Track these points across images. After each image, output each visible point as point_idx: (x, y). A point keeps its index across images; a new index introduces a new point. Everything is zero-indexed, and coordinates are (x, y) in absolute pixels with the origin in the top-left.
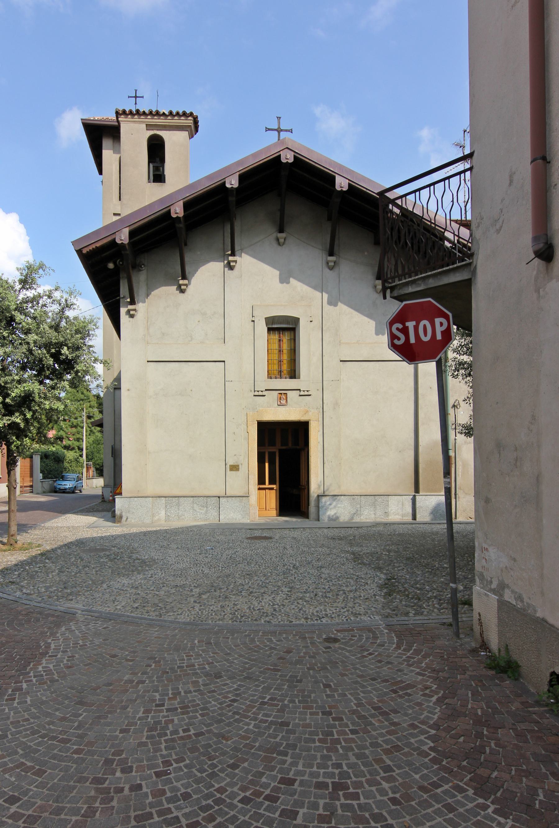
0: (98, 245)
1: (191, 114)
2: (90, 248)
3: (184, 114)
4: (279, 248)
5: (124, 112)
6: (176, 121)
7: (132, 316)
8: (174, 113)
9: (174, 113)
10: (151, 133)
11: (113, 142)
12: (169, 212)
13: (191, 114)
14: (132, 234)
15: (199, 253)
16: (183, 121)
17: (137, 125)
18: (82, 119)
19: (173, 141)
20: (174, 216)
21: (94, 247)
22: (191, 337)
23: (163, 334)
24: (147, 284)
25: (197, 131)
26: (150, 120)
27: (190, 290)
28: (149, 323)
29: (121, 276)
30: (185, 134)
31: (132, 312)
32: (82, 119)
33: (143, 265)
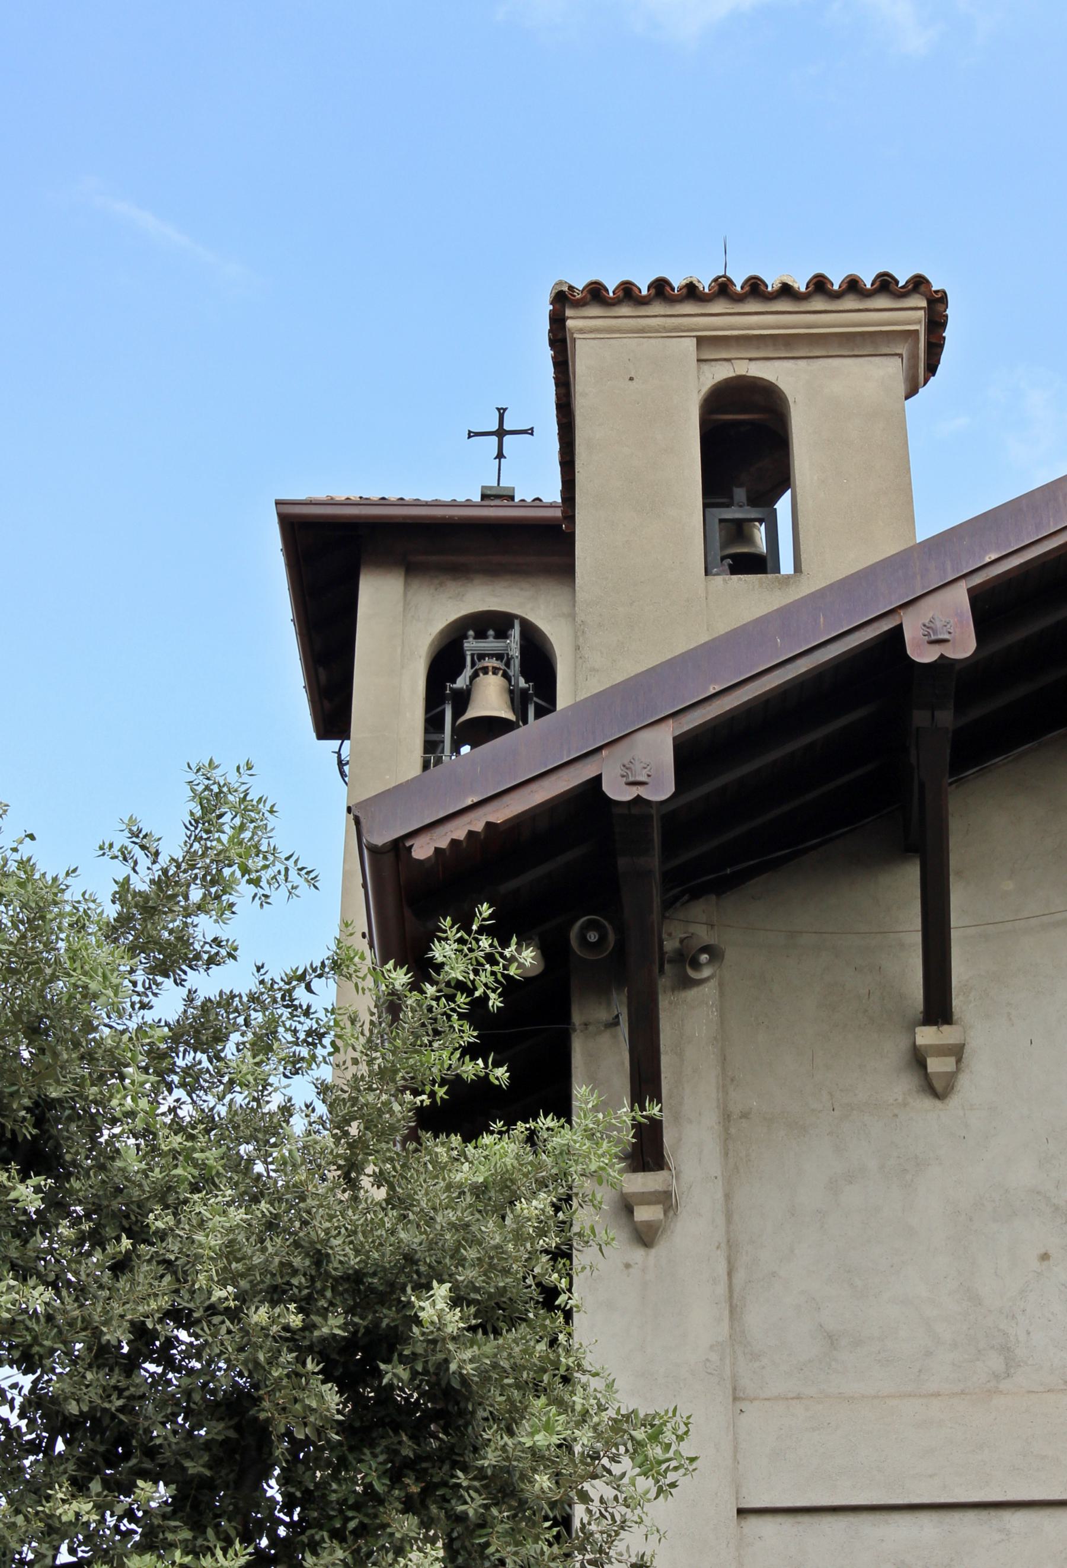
0: (501, 813)
1: (919, 283)
2: (458, 831)
3: (885, 284)
4: (938, 1103)
5: (596, 293)
6: (849, 317)
7: (645, 1237)
8: (836, 282)
9: (836, 282)
10: (722, 372)
11: (407, 584)
12: (896, 634)
13: (919, 283)
14: (690, 755)
15: (1009, 885)
16: (882, 314)
17: (652, 345)
18: (278, 503)
19: (822, 399)
20: (923, 654)
21: (460, 835)
22: (1006, 1350)
23: (832, 1340)
24: (723, 1060)
25: (932, 368)
26: (721, 319)
27: (977, 1083)
28: (740, 1276)
29: (577, 1018)
30: (889, 371)
31: (643, 1214)
32: (278, 503)
33: (705, 949)
